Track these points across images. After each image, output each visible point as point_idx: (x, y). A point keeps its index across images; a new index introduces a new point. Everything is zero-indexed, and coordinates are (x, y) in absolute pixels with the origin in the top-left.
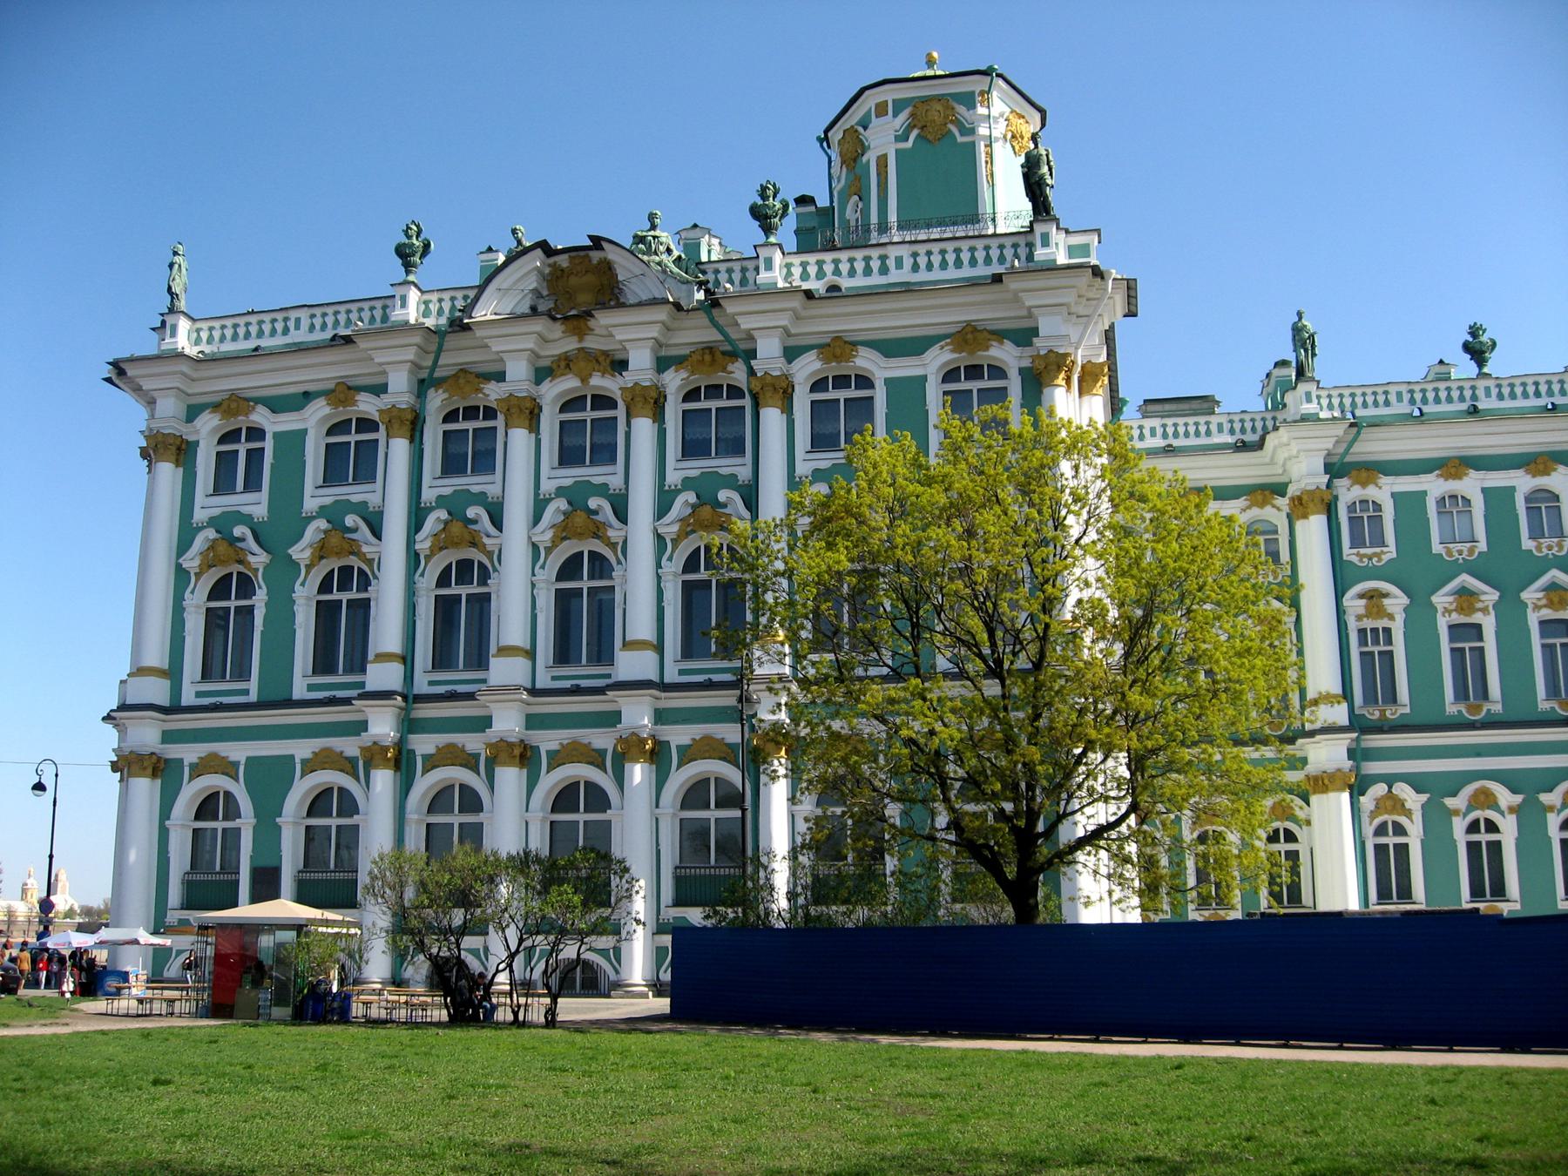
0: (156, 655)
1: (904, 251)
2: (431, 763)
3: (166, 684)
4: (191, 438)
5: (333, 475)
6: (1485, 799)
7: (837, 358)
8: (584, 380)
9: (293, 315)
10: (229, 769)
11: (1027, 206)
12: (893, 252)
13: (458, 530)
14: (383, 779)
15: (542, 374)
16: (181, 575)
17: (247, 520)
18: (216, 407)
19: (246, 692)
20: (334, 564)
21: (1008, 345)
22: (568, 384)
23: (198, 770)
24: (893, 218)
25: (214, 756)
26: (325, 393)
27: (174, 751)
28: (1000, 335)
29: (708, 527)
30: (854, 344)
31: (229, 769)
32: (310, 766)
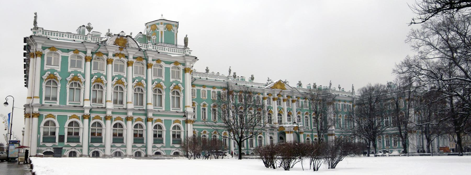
0: (37, 94)
1: (168, 48)
2: (94, 119)
3: (39, 100)
4: (43, 53)
5: (72, 66)
6: (205, 132)
7: (158, 62)
8: (120, 58)
9: (65, 34)
10: (54, 117)
11: (184, 45)
12: (166, 48)
13: (120, 82)
14: (86, 121)
15: (114, 55)
16: (42, 79)
17: (56, 71)
18: (49, 48)
19: (80, 104)
20: (138, 87)
21: (181, 65)
22: (118, 58)
23: (46, 117)
24: (163, 42)
25: (139, 118)
26: (74, 51)
27: (41, 113)
28: (180, 64)
29: (139, 85)
30: (161, 61)
31: (54, 117)
32: (71, 117)
